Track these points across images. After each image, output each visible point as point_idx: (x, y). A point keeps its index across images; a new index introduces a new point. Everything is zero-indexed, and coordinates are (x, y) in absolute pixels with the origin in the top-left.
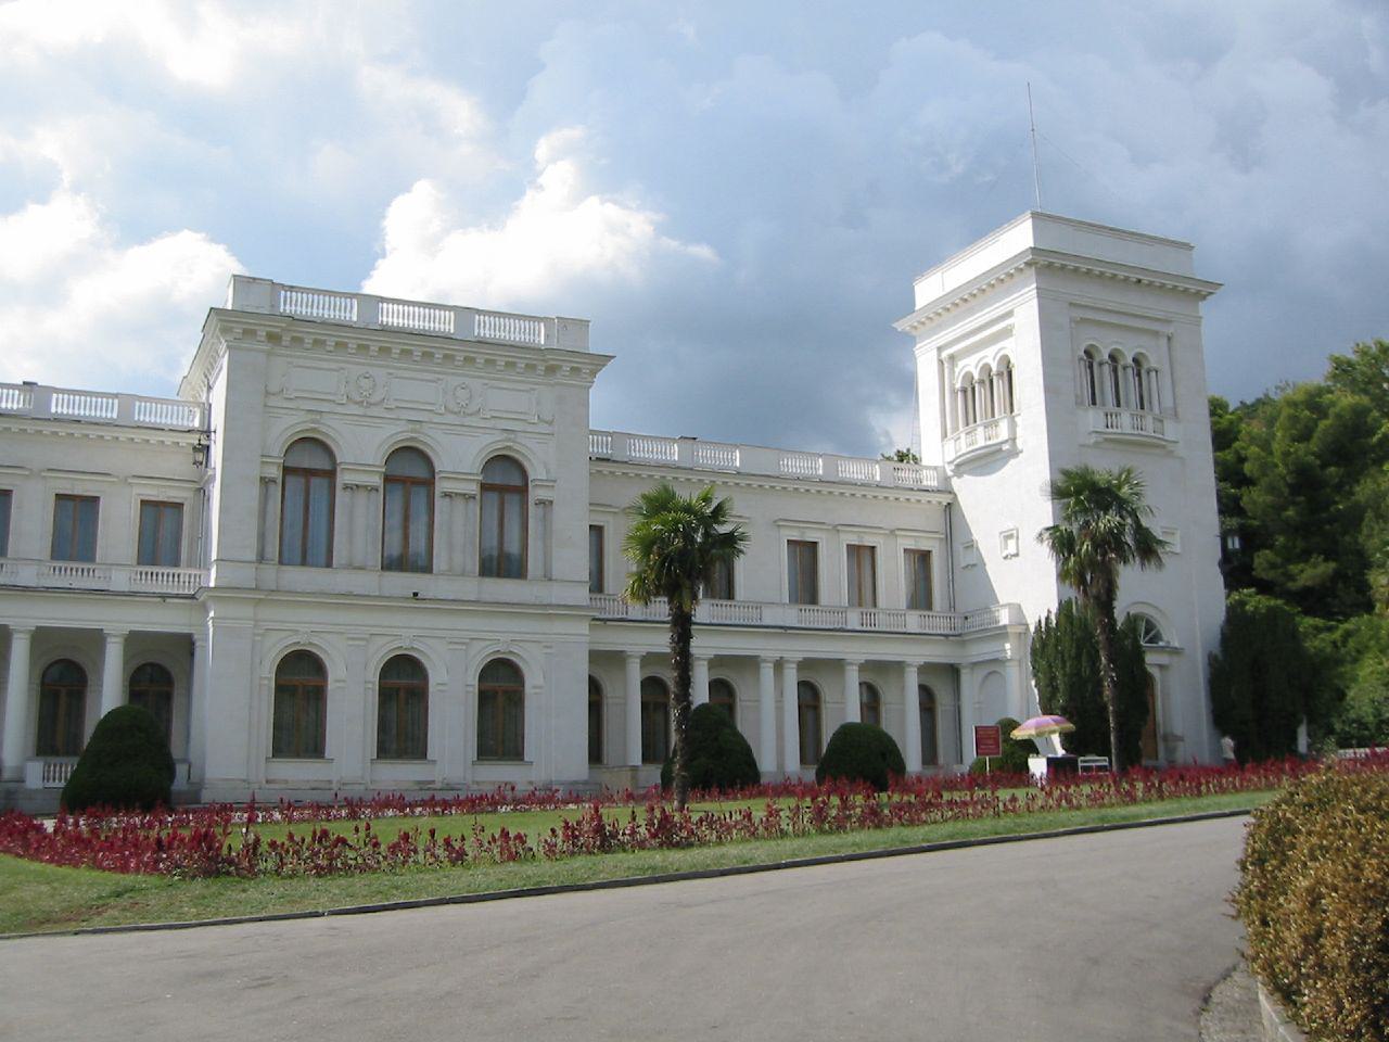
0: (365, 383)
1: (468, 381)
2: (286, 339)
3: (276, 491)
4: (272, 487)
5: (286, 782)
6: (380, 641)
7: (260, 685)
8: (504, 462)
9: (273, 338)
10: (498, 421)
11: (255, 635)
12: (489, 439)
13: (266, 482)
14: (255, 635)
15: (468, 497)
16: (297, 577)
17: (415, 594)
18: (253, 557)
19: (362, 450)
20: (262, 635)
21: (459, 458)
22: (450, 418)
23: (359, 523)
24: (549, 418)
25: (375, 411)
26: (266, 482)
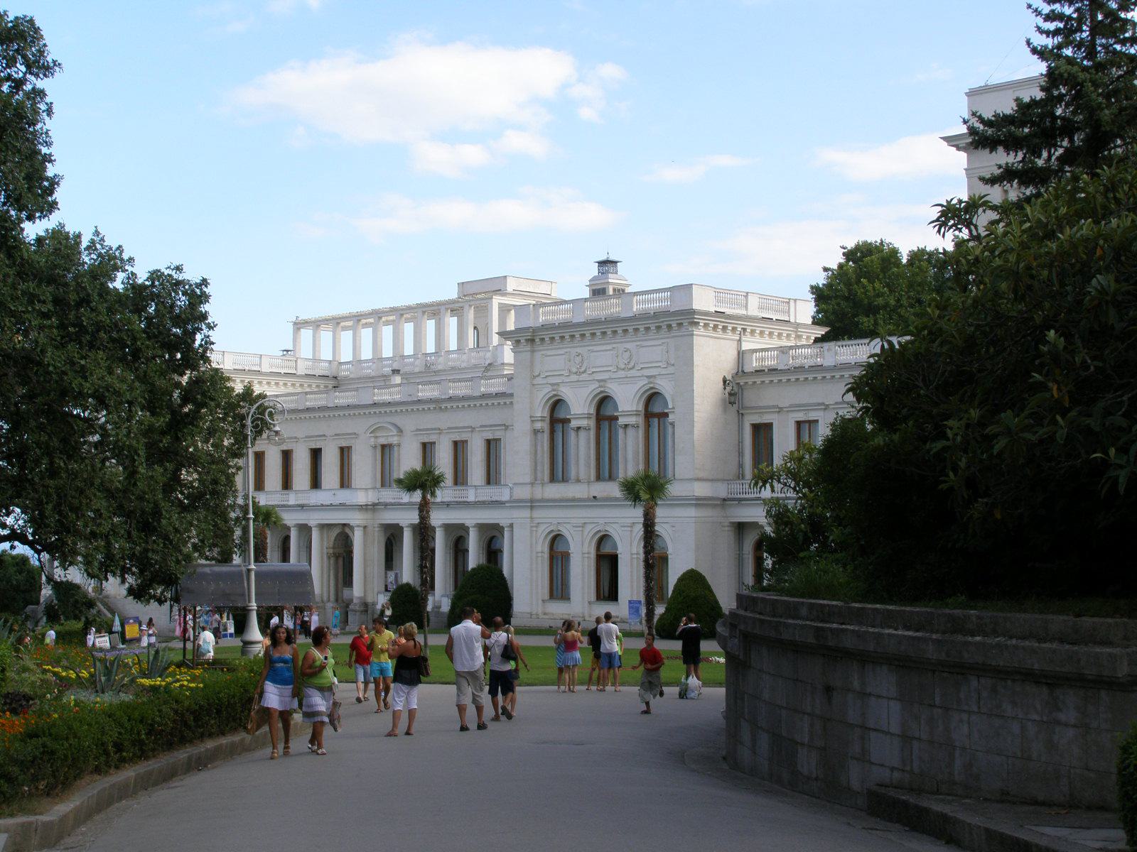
0: (578, 359)
1: (628, 346)
2: (537, 340)
3: (546, 436)
4: (539, 435)
5: (553, 614)
6: (591, 526)
7: (537, 557)
8: (652, 397)
9: (532, 341)
10: (645, 370)
11: (532, 527)
12: (641, 383)
13: (536, 432)
14: (532, 527)
15: (636, 427)
16: (555, 491)
17: (595, 497)
18: (528, 479)
19: (580, 405)
20: (536, 527)
21: (628, 401)
22: (622, 374)
23: (582, 449)
24: (672, 362)
25: (584, 377)
26: (536, 432)
